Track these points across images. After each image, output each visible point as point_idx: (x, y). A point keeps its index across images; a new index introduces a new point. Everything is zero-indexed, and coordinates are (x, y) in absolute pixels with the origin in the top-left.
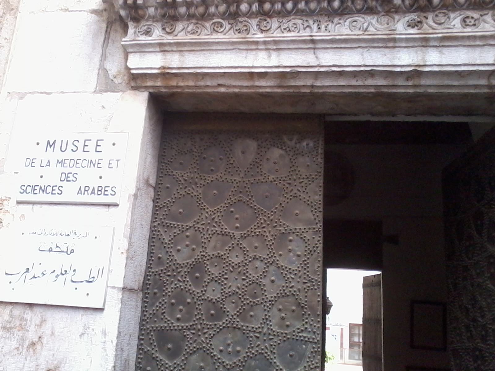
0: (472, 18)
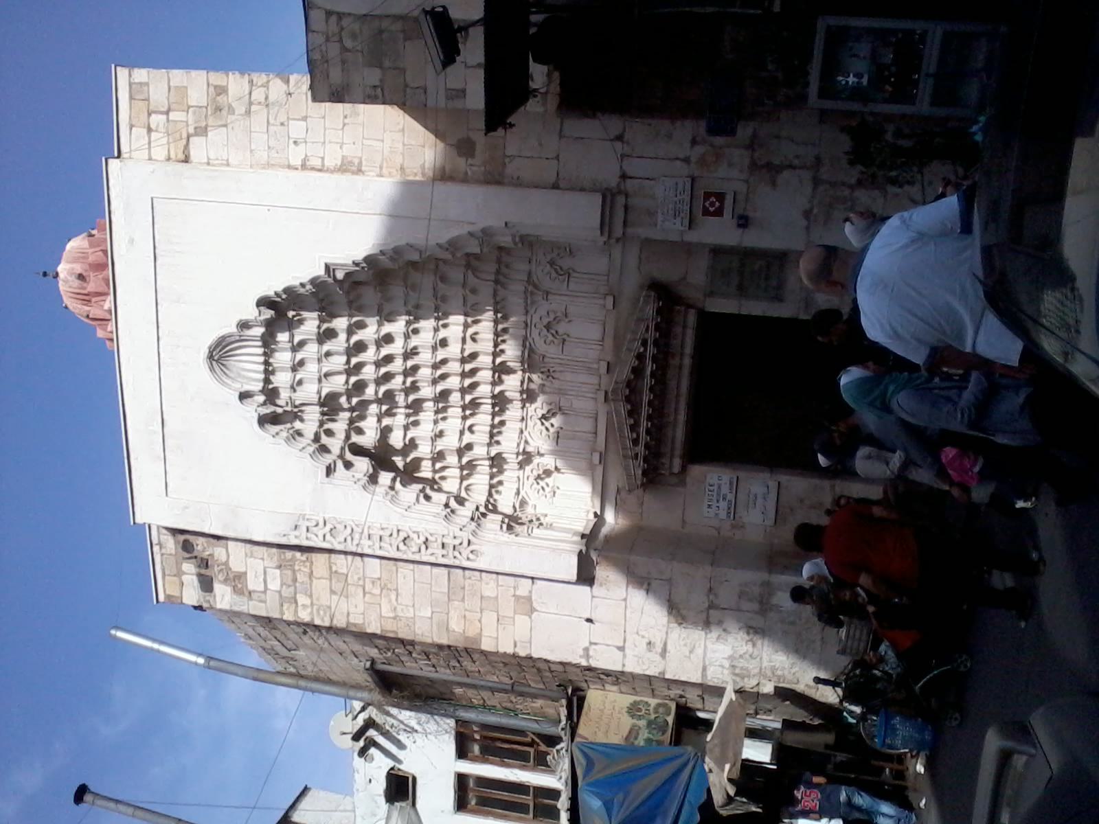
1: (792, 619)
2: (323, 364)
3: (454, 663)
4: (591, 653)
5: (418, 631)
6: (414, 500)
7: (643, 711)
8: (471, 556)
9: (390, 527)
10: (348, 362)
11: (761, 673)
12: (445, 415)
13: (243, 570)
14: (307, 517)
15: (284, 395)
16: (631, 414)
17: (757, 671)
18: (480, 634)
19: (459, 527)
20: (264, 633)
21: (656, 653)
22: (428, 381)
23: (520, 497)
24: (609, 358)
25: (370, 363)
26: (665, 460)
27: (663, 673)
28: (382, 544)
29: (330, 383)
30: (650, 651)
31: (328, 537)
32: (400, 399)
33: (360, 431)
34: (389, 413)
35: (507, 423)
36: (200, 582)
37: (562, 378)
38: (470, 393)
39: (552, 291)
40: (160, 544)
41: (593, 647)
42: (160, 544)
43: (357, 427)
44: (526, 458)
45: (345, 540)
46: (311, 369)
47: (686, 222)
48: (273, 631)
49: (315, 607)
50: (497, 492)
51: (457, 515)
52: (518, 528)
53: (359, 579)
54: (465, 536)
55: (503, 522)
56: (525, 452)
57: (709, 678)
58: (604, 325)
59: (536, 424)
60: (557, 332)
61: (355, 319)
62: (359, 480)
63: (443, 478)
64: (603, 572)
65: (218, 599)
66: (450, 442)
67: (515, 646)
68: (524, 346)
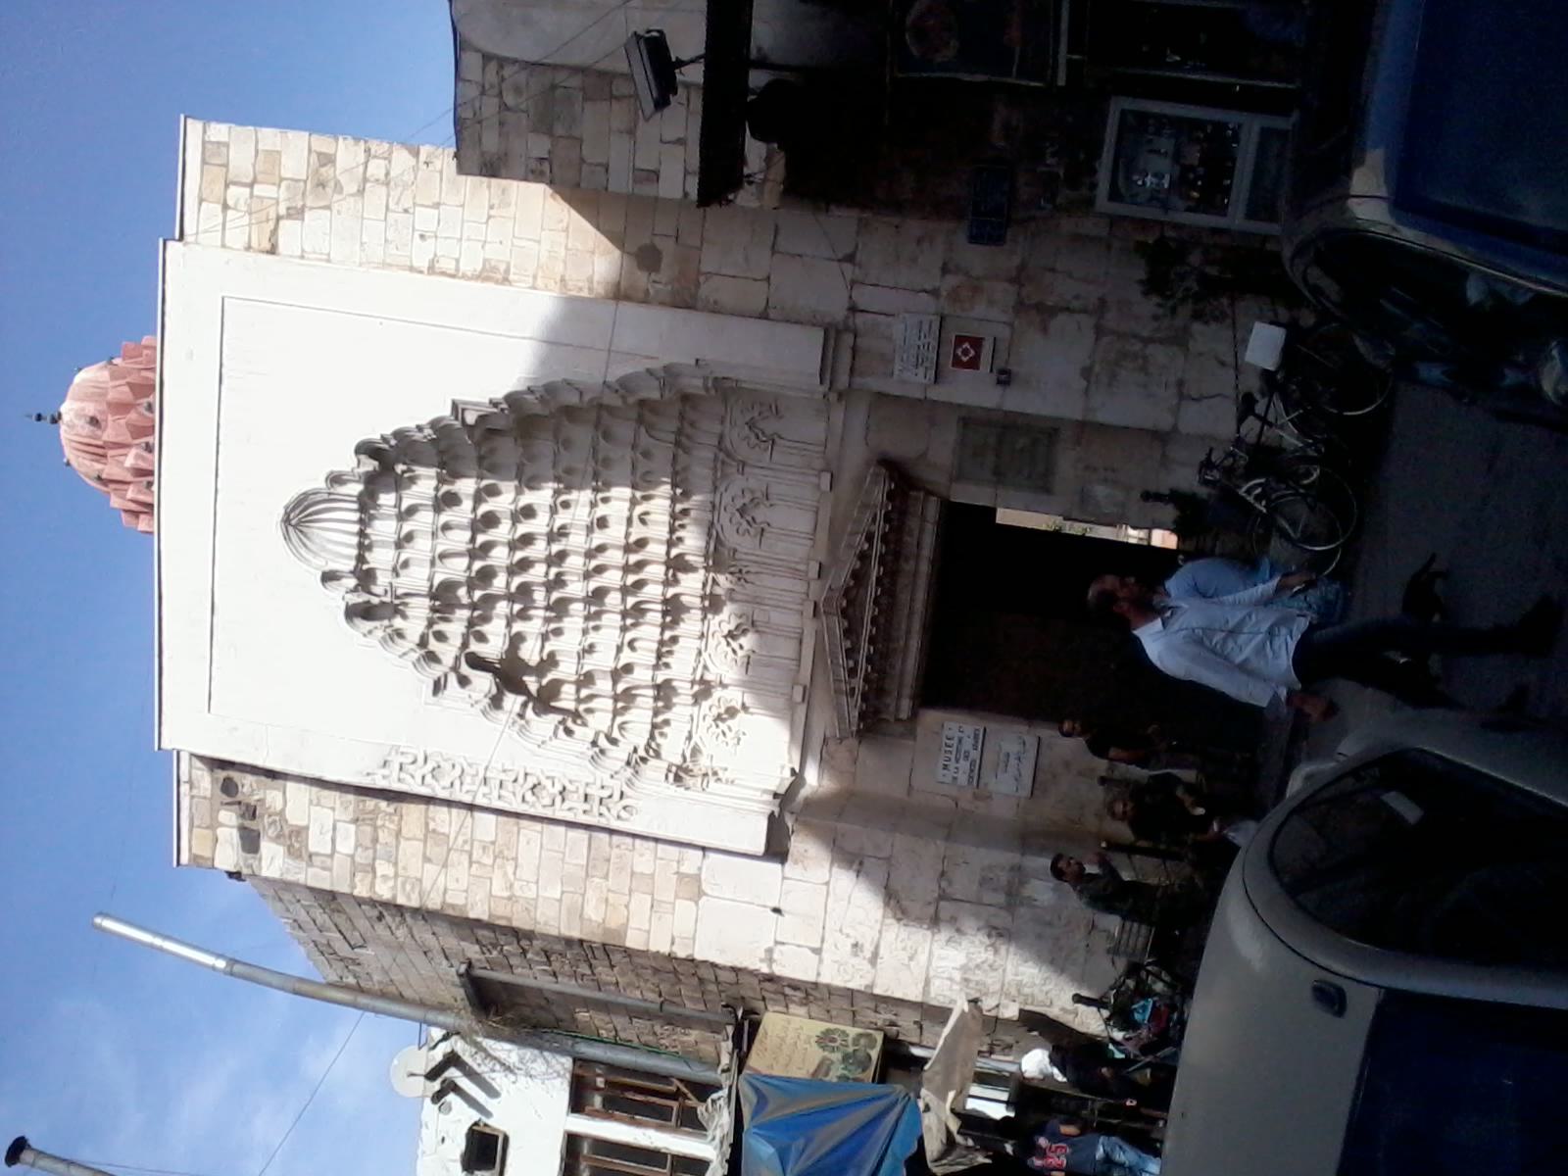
1: (1048, 918)
2: (439, 541)
3: (584, 969)
4: (776, 956)
5: (540, 918)
6: (551, 734)
7: (839, 1042)
8: (623, 814)
9: (516, 768)
10: (473, 540)
11: (1003, 992)
13: (304, 823)
14: (401, 750)
15: (383, 579)
16: (848, 633)
17: (997, 987)
18: (626, 926)
19: (610, 772)
20: (322, 918)
21: (864, 958)
22: (578, 574)
23: (692, 743)
24: (822, 558)
25: (503, 544)
26: (890, 701)
27: (871, 986)
28: (503, 792)
29: (446, 568)
30: (856, 955)
31: (429, 779)
32: (539, 596)
33: (482, 638)
34: (523, 615)
35: (681, 639)
36: (242, 837)
37: (758, 583)
38: (634, 594)
39: (750, 462)
40: (190, 782)
41: (779, 947)
42: (190, 782)
43: (478, 632)
44: (704, 689)
45: (452, 784)
46: (422, 547)
47: (931, 373)
48: (336, 914)
49: (400, 880)
50: (662, 734)
51: (609, 758)
52: (688, 780)
53: (465, 842)
54: (616, 785)
55: (669, 771)
56: (702, 681)
57: (933, 995)
58: (817, 513)
59: (719, 643)
60: (753, 519)
61: (485, 482)
62: (477, 702)
63: (589, 711)
64: (801, 845)
65: (264, 863)
66: (603, 660)
67: (673, 943)
68: (709, 535)
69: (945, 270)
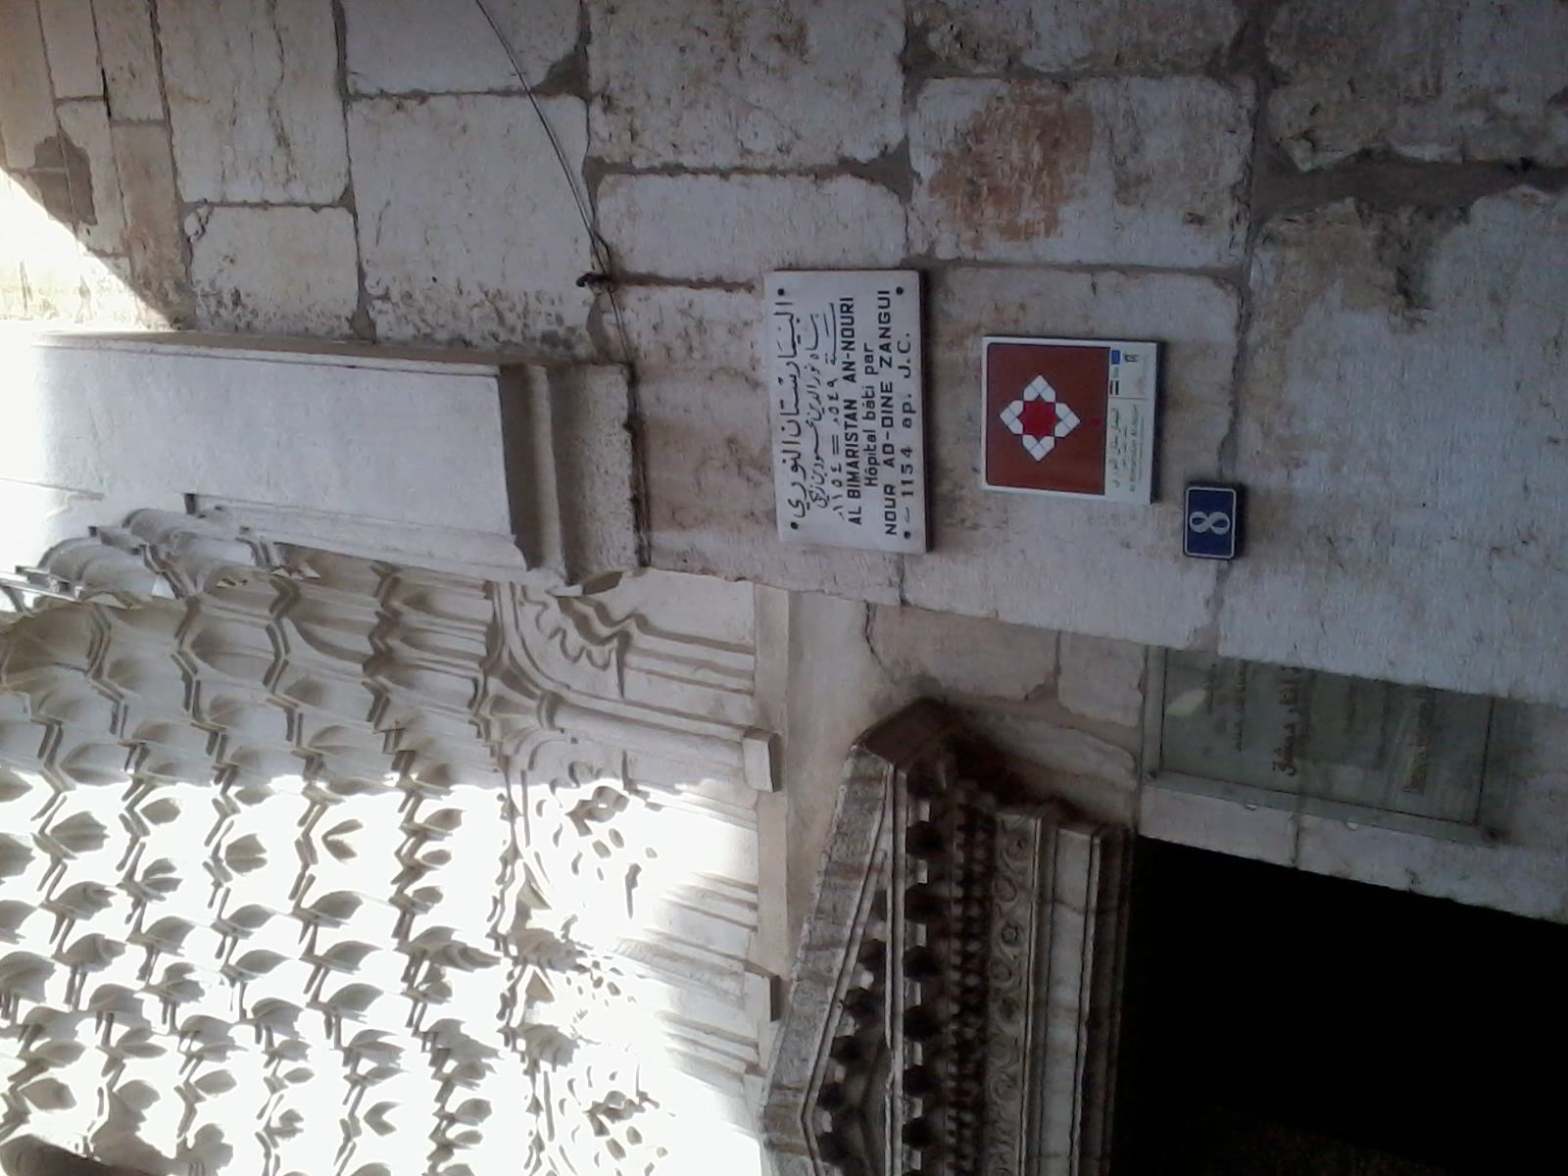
0: (1004, 929)
12: (300, 1064)
33: (57, 1096)
34: (138, 1043)
43: (52, 1081)
47: (912, 509)
69: (918, 64)
